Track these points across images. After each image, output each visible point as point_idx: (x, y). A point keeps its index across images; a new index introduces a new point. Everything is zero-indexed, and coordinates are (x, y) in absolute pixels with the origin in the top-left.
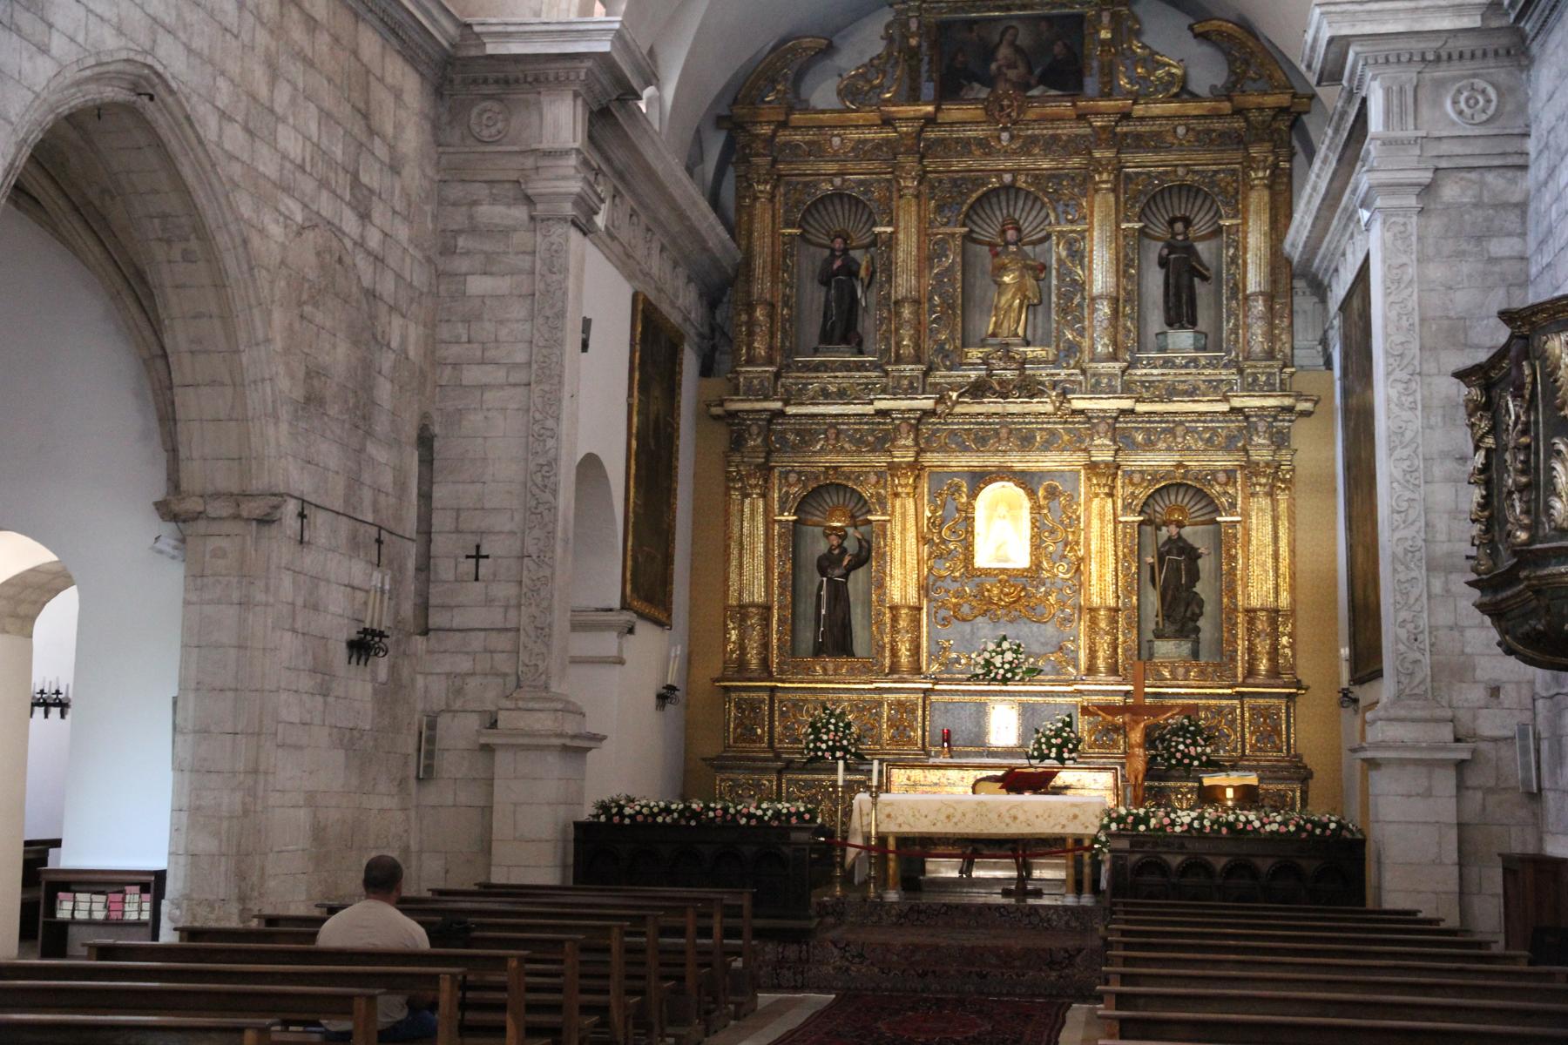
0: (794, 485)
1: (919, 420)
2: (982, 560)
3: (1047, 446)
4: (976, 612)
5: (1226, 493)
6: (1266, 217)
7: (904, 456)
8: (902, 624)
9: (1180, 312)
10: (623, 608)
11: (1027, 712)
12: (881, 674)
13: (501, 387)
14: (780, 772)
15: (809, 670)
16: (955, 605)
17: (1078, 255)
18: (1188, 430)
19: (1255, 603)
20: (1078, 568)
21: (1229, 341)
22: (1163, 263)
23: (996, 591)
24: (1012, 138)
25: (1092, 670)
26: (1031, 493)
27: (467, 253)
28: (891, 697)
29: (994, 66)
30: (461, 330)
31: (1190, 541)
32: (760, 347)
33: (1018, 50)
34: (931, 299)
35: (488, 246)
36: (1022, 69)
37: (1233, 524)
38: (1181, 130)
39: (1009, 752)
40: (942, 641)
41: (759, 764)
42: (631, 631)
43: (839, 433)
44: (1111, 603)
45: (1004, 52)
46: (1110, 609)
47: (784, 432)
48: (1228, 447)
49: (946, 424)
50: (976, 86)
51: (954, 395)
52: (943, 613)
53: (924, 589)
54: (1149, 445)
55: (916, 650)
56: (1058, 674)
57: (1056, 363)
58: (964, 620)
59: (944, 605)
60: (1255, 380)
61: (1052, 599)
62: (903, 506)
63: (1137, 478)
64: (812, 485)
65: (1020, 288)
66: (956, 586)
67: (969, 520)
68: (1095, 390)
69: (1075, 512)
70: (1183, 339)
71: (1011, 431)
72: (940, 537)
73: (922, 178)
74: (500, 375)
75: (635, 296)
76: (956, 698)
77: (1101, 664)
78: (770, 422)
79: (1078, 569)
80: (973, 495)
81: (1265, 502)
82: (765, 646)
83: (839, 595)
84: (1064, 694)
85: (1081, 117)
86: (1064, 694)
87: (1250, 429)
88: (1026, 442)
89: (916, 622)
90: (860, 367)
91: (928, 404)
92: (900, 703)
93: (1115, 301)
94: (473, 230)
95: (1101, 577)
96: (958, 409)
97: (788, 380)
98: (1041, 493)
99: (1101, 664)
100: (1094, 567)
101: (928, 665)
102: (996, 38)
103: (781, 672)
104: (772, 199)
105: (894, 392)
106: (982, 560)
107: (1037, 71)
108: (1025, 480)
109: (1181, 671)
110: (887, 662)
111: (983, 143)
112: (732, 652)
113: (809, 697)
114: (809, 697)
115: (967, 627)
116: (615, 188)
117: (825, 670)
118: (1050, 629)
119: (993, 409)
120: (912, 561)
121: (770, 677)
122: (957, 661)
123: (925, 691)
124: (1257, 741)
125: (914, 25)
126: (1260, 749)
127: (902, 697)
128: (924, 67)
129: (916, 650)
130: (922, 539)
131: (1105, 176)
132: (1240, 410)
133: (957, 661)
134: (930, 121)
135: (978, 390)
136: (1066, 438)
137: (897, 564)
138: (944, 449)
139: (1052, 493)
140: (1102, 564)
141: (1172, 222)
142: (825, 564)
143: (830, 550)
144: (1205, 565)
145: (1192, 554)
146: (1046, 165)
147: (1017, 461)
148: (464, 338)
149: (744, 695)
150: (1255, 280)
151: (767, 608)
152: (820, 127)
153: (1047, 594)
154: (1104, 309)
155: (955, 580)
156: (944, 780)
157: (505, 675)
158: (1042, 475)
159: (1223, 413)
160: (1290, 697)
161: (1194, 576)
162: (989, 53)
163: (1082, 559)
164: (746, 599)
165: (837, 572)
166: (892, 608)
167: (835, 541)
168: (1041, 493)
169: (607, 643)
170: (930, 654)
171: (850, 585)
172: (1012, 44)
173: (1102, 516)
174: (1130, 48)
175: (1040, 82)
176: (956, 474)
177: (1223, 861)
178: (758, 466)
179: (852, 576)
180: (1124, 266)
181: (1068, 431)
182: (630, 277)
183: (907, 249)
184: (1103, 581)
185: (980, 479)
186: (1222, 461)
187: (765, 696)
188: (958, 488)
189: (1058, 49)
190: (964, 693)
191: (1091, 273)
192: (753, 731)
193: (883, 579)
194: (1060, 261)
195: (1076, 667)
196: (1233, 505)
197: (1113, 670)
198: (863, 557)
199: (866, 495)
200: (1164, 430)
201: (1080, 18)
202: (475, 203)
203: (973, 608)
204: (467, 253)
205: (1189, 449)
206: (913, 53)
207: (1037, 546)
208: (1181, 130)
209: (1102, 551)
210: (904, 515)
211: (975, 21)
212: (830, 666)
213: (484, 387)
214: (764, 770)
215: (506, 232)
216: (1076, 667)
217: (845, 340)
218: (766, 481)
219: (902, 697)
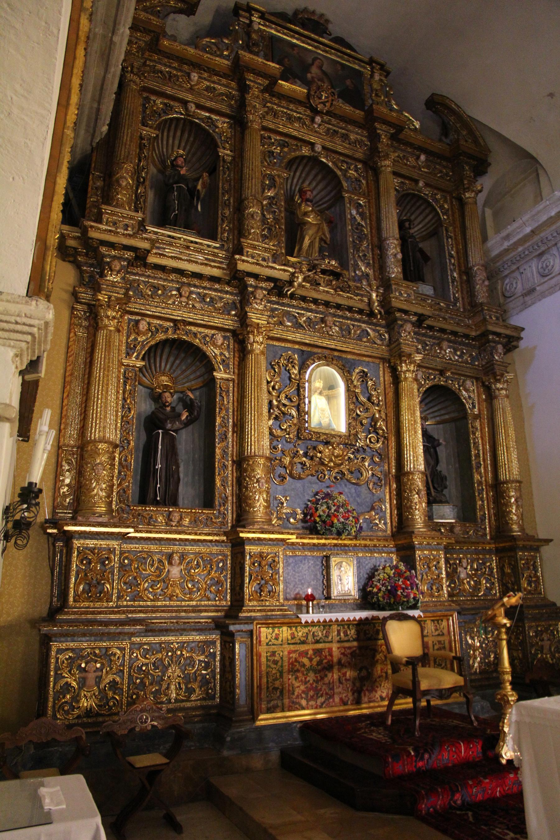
0: (144, 334)
4: (307, 472)
5: (470, 397)
33: (324, 73)
38: (423, 157)
41: (112, 628)
43: (191, 293)
45: (314, 70)
49: (283, 305)
58: (300, 478)
64: (161, 336)
65: (319, 227)
72: (279, 402)
80: (303, 367)
96: (300, 292)
98: (355, 377)
102: (310, 61)
112: (65, 496)
115: (298, 484)
117: (169, 519)
122: (294, 514)
127: (265, 549)
139: (364, 375)
149: (91, 543)
153: (363, 459)
162: (307, 68)
165: (177, 425)
168: (355, 377)
172: (320, 68)
176: (289, 349)
181: (374, 330)
198: (203, 413)
200: (434, 343)
205: (450, 359)
207: (353, 418)
208: (423, 157)
219: (265, 549)
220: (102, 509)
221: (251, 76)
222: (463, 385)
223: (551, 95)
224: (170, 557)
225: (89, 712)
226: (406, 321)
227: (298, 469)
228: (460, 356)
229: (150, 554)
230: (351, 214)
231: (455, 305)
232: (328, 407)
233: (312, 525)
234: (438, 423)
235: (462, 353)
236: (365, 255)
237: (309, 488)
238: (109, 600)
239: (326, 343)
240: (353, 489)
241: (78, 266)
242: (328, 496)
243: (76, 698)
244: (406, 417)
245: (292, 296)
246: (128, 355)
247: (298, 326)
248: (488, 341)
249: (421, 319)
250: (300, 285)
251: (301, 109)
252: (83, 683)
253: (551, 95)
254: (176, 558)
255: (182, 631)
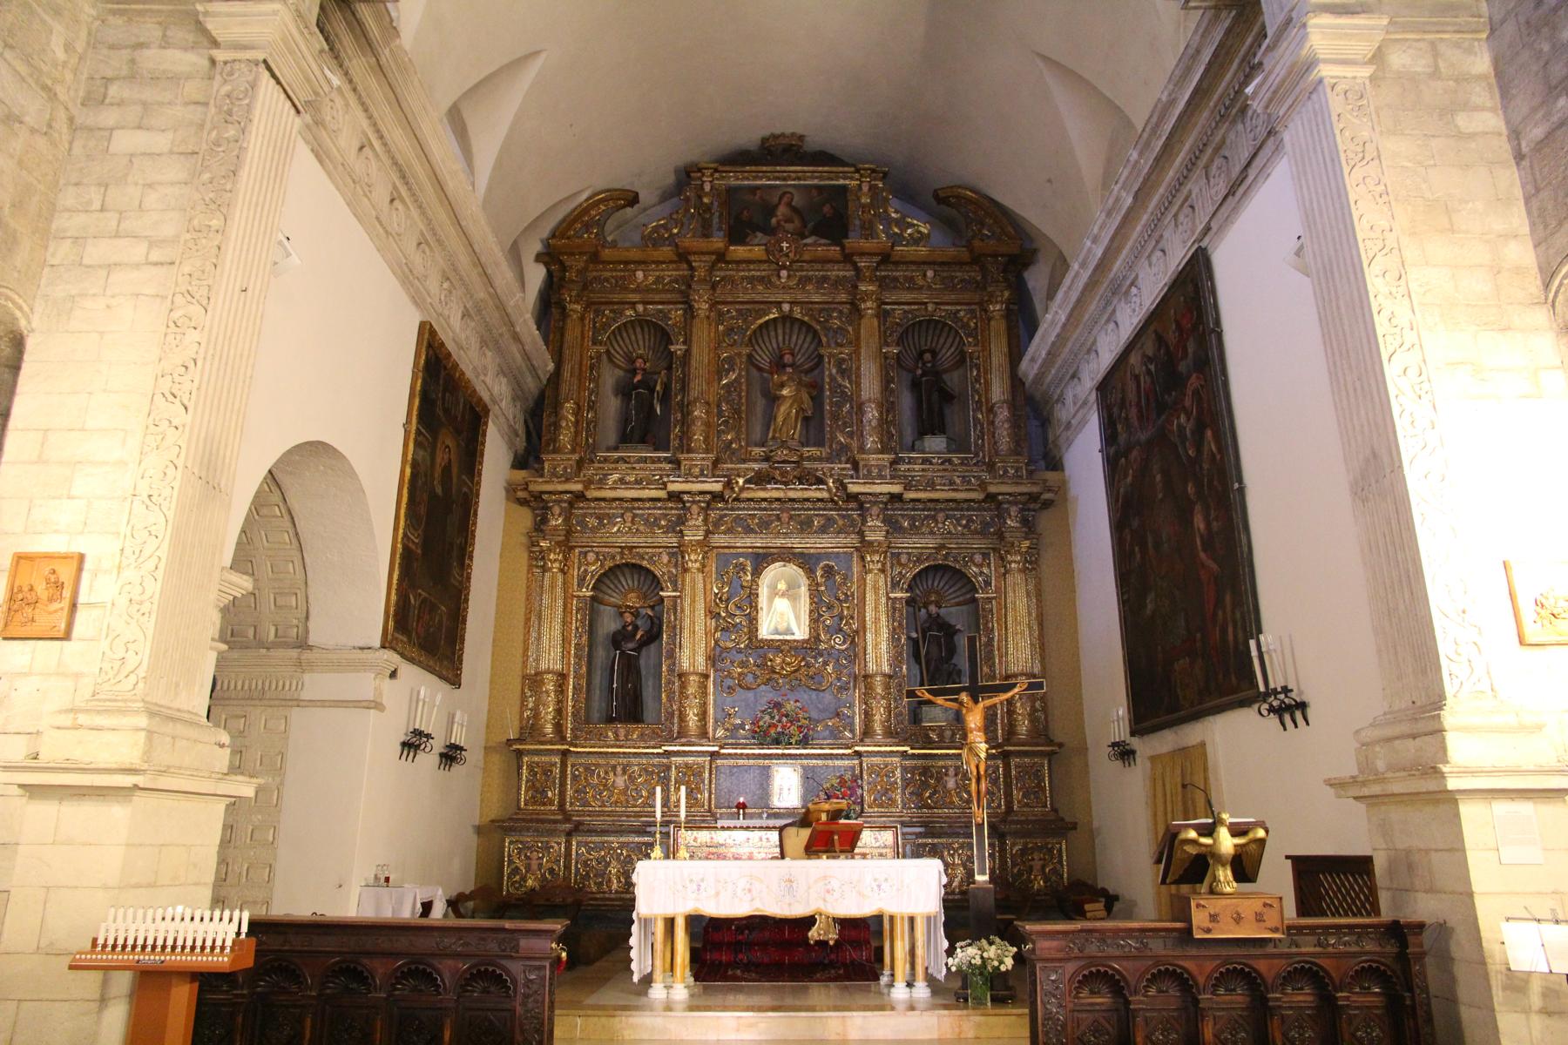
1: (708, 503)
2: (765, 631)
3: (823, 530)
6: (1004, 341)
7: (693, 535)
8: (691, 690)
9: (930, 421)
10: (383, 647)
11: (808, 777)
12: (671, 740)
13: (137, 266)
14: (569, 834)
15: (601, 736)
16: (740, 674)
17: (848, 370)
18: (947, 517)
19: (1013, 669)
20: (855, 639)
21: (976, 444)
22: (915, 385)
23: (778, 660)
24: (789, 276)
25: (867, 732)
26: (810, 572)
27: (121, 103)
28: (679, 760)
29: (774, 221)
30: (95, 196)
31: (947, 619)
32: (565, 438)
33: (794, 209)
34: (719, 406)
35: (149, 94)
36: (797, 223)
37: (989, 600)
38: (930, 274)
39: (789, 812)
40: (727, 708)
41: (548, 826)
42: (393, 675)
43: (635, 516)
44: (886, 669)
45: (782, 210)
46: (885, 675)
47: (585, 515)
48: (983, 533)
49: (732, 509)
50: (759, 235)
51: (741, 481)
52: (729, 682)
53: (712, 659)
54: (914, 530)
55: (703, 716)
56: (836, 738)
57: (829, 460)
59: (730, 675)
60: (1006, 472)
61: (830, 669)
62: (693, 580)
63: (904, 559)
64: (609, 564)
65: (796, 399)
66: (742, 657)
67: (753, 597)
68: (869, 478)
69: (849, 588)
70: (936, 443)
71: (791, 517)
73: (713, 305)
74: (138, 251)
75: (422, 325)
76: (741, 762)
77: (878, 728)
78: (571, 504)
79: (853, 642)
80: (757, 573)
81: (1019, 578)
82: (559, 712)
83: (630, 668)
84: (842, 757)
85: (848, 258)
86: (842, 757)
87: (1001, 514)
88: (805, 526)
89: (703, 688)
90: (659, 460)
91: (717, 487)
92: (687, 765)
93: (880, 406)
94: (132, 77)
95: (876, 645)
96: (745, 495)
97: (589, 471)
98: (819, 573)
99: (878, 728)
100: (869, 636)
101: (715, 730)
102: (776, 200)
103: (575, 737)
104: (582, 319)
105: (689, 476)
106: (765, 631)
107: (810, 225)
108: (806, 561)
109: (948, 733)
110: (676, 728)
111: (761, 280)
113: (601, 761)
114: (601, 761)
115: (750, 695)
116: (395, 187)
117: (616, 735)
118: (827, 697)
119: (775, 494)
120: (700, 628)
121: (563, 739)
122: (742, 726)
123: (713, 755)
124: (1024, 796)
125: (707, 187)
126: (1027, 805)
127: (690, 760)
128: (716, 220)
129: (703, 716)
130: (712, 614)
131: (869, 304)
132: (991, 497)
133: (742, 726)
134: (721, 257)
135: (760, 479)
136: (841, 522)
137: (686, 633)
138: (729, 531)
139: (829, 571)
140: (877, 633)
141: (921, 354)
142: (617, 640)
143: (624, 627)
144: (962, 642)
145: (949, 631)
146: (816, 298)
147: (797, 543)
148: (97, 205)
150: (998, 391)
151: (562, 676)
152: (626, 263)
153: (826, 663)
154: (872, 413)
155: (740, 651)
156: (730, 841)
157: (77, 676)
158: (818, 557)
159: (979, 502)
160: (1050, 755)
161: (952, 650)
162: (770, 210)
163: (857, 632)
164: (543, 666)
165: (631, 645)
166: (680, 676)
167: (628, 618)
168: (819, 573)
169: (365, 684)
170: (716, 721)
171: (642, 662)
172: (789, 204)
173: (876, 589)
174: (886, 211)
175: (812, 233)
176: (741, 555)
177: (1209, 966)
178: (558, 543)
179: (644, 652)
180: (886, 382)
181: (843, 517)
182: (417, 301)
183: (701, 357)
184: (879, 650)
185: (761, 560)
186: (978, 543)
187: (557, 759)
188: (744, 570)
189: (827, 208)
190: (748, 756)
191: (858, 384)
192: (544, 792)
193: (673, 650)
194: (832, 378)
195: (852, 731)
196: (987, 583)
197: (889, 733)
199: (658, 573)
200: (927, 517)
201: (844, 188)
202: (140, 46)
203: (756, 677)
204: (121, 103)
206: (708, 208)
207: (815, 620)
208: (930, 274)
209: (877, 620)
210: (693, 588)
211: (758, 188)
212: (622, 732)
213: (110, 267)
214: (552, 833)
215: (175, 79)
216: (852, 731)
217: (643, 441)
218: (566, 559)
220: (549, 729)
221: (696, 257)
222: (972, 560)
223: (1049, 181)
224: (614, 768)
225: (533, 890)
226: (875, 503)
227: (750, 678)
228: (964, 527)
229: (598, 765)
230: (831, 375)
231: (977, 455)
232: (783, 612)
233: (762, 736)
234: (958, 604)
235: (970, 520)
236: (845, 423)
237: (766, 694)
238: (551, 803)
239: (779, 542)
240: (814, 694)
241: (534, 509)
242: (778, 706)
243: (524, 879)
244: (869, 615)
245: (736, 499)
246: (580, 586)
247: (749, 530)
248: (1001, 503)
249: (895, 498)
250: (742, 489)
251: (765, 266)
252: (528, 868)
253: (1049, 181)
254: (619, 769)
255: (620, 832)
